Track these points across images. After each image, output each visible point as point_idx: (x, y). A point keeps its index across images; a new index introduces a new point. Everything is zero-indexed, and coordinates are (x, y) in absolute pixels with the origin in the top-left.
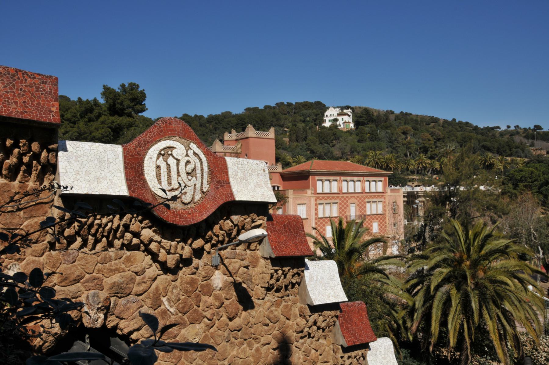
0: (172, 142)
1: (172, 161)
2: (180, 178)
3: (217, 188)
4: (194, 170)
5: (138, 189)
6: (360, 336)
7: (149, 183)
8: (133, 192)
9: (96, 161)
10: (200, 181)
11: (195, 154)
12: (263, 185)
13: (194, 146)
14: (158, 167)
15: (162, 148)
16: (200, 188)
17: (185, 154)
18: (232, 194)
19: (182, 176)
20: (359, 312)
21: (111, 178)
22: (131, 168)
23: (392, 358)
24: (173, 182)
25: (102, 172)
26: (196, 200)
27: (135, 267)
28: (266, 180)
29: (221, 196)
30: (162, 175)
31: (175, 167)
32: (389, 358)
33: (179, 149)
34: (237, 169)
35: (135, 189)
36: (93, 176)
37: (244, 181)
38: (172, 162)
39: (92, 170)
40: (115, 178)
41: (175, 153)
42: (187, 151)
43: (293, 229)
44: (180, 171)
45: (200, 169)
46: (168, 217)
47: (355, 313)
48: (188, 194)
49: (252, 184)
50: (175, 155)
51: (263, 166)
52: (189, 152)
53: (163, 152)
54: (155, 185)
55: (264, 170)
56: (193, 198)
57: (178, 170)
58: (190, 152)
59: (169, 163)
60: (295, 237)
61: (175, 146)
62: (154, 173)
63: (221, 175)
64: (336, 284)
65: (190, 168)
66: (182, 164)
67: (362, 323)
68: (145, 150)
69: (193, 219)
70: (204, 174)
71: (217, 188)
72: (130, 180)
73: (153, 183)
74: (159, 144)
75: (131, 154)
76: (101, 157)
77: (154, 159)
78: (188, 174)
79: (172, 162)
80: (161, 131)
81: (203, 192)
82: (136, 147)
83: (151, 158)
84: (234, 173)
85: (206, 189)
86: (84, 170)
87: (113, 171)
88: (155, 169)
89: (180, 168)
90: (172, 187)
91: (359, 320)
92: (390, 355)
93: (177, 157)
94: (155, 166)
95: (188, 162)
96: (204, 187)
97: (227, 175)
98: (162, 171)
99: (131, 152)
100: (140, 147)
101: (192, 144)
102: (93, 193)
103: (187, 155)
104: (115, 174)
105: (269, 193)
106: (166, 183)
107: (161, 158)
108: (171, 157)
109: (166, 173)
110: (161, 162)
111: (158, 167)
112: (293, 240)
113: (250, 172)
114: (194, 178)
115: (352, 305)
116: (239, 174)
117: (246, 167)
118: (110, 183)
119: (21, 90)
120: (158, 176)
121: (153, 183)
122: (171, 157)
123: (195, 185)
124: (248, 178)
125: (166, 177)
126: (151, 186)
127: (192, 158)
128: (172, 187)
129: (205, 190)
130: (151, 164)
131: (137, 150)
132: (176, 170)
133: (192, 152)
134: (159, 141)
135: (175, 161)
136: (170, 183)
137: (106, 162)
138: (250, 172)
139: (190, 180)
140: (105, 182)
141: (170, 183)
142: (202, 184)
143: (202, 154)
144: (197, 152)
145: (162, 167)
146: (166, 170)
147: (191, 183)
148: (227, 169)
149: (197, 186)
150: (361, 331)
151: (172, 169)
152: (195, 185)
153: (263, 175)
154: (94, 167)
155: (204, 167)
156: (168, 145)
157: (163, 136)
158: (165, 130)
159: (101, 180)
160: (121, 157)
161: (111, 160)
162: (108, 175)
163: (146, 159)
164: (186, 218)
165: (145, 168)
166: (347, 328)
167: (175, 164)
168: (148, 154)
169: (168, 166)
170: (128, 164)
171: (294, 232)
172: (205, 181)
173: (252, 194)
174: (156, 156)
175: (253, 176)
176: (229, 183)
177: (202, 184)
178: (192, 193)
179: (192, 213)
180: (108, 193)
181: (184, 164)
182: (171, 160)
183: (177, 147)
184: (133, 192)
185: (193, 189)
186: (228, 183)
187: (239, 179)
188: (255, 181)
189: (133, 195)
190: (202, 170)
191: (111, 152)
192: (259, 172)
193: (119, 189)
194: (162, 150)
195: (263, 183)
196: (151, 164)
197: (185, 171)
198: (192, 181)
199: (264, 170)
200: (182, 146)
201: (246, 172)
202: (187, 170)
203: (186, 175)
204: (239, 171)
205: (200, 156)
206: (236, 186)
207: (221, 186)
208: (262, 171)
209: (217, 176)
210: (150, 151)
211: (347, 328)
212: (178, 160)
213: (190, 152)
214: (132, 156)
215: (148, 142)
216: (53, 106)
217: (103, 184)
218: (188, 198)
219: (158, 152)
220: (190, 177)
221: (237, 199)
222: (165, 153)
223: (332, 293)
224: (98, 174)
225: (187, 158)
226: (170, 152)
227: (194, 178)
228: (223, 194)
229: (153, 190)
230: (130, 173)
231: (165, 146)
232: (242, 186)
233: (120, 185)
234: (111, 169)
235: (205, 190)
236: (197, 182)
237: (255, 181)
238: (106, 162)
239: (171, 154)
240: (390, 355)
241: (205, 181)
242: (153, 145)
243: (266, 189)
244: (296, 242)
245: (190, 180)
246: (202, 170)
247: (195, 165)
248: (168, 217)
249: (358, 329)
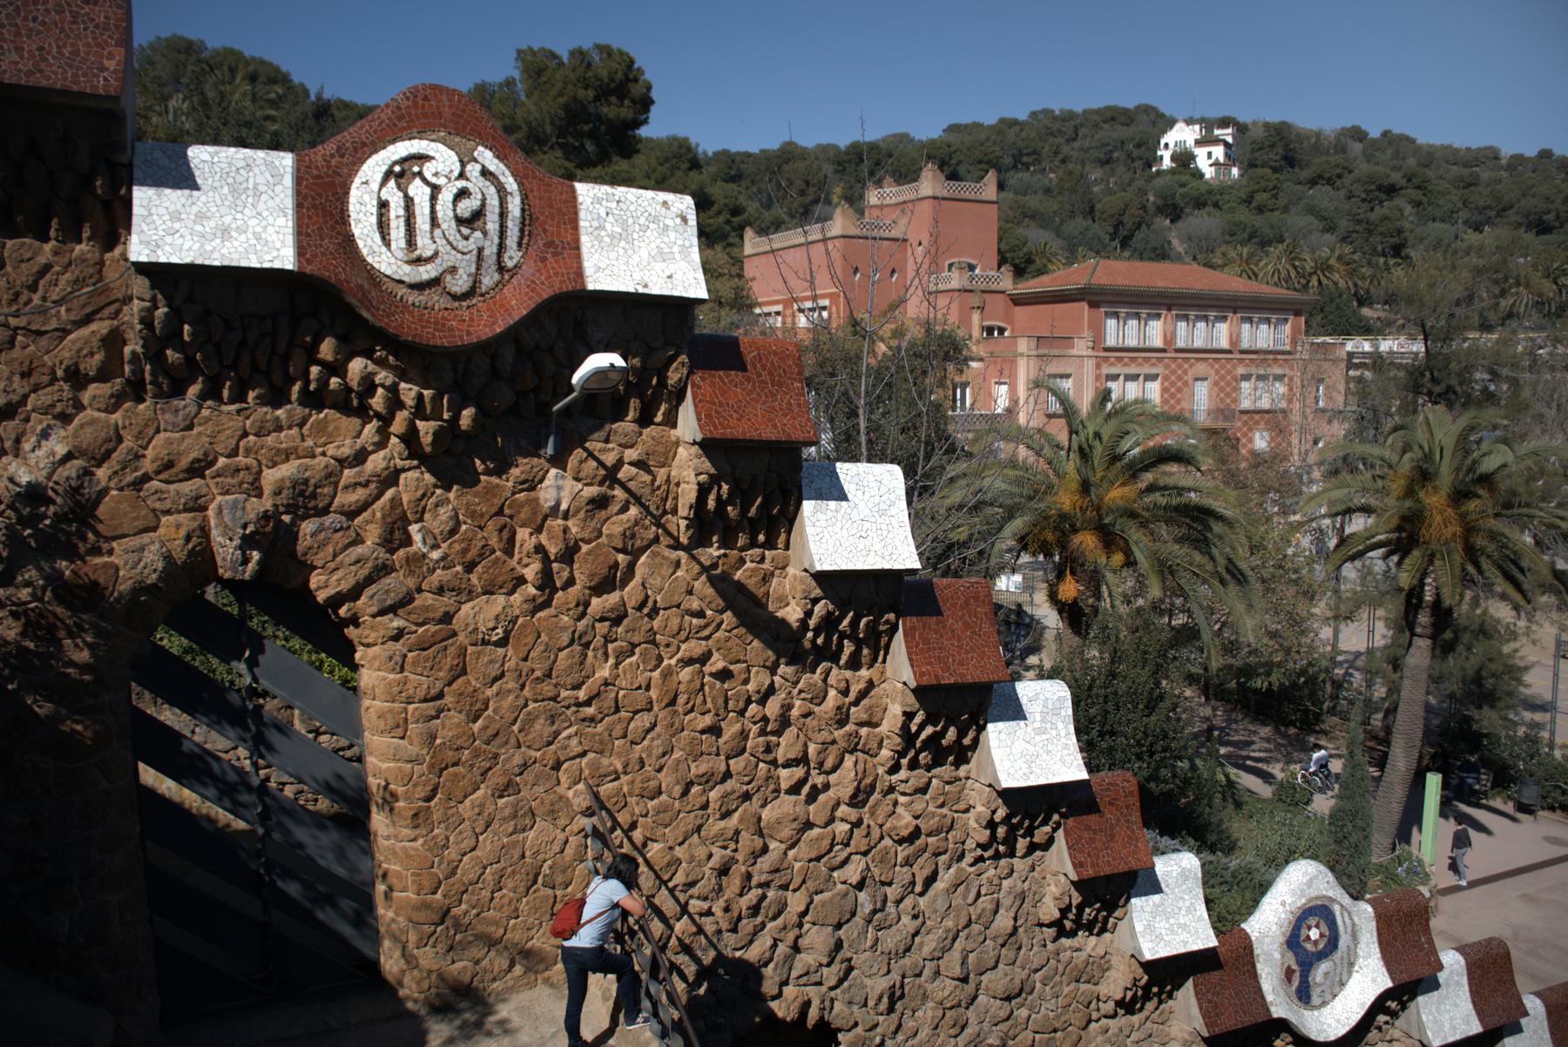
0: (424, 143)
1: (418, 191)
2: (437, 232)
3: (544, 260)
4: (478, 215)
5: (323, 254)
6: (961, 664)
7: (360, 244)
8: (309, 262)
9: (226, 190)
10: (496, 241)
11: (485, 173)
12: (678, 256)
13: (486, 156)
14: (383, 205)
15: (396, 157)
16: (494, 257)
17: (456, 173)
18: (580, 274)
19: (444, 226)
20: (967, 603)
21: (259, 229)
22: (315, 207)
23: (1063, 733)
24: (420, 242)
25: (239, 216)
26: (484, 289)
27: (339, 447)
28: (687, 243)
29: (549, 277)
30: (393, 224)
31: (427, 205)
32: (1054, 732)
33: (443, 159)
34: (603, 214)
35: (316, 256)
36: (212, 224)
37: (623, 244)
38: (419, 191)
39: (214, 209)
40: (270, 230)
41: (429, 170)
42: (463, 164)
43: (770, 374)
44: (440, 215)
45: (497, 210)
46: (401, 325)
47: (954, 605)
48: (461, 271)
49: (644, 253)
50: (428, 175)
51: (683, 207)
52: (469, 167)
53: (397, 169)
54: (376, 248)
55: (685, 220)
56: (476, 283)
57: (433, 212)
58: (473, 170)
59: (411, 193)
60: (773, 395)
61: (431, 153)
62: (374, 219)
63: (558, 225)
64: (895, 524)
65: (466, 208)
66: (446, 196)
67: (974, 632)
68: (354, 164)
69: (469, 333)
70: (510, 224)
71: (544, 260)
72: (308, 235)
73: (369, 242)
74: (391, 148)
75: (315, 172)
76: (239, 178)
77: (375, 186)
78: (460, 221)
79: (419, 191)
80: (400, 118)
81: (501, 268)
82: (332, 156)
83: (366, 183)
84: (595, 224)
85: (515, 261)
86: (195, 209)
87: (265, 214)
88: (374, 210)
89: (438, 208)
90: (417, 253)
91: (967, 626)
92: (1060, 725)
93: (434, 180)
94: (375, 202)
95: (462, 194)
96: (506, 256)
97: (576, 228)
98: (392, 215)
99: (317, 168)
100: (342, 156)
101: (480, 148)
102: (207, 263)
103: (462, 176)
104: (271, 220)
105: (691, 275)
106: (403, 244)
107: (392, 183)
108: (418, 181)
109: (402, 220)
110: (392, 194)
111: (383, 205)
112: (764, 403)
113: (642, 221)
114: (478, 234)
115: (949, 586)
116: (608, 227)
117: (632, 208)
118: (254, 242)
119: (35, 19)
120: (383, 227)
121: (369, 242)
122: (418, 181)
123: (480, 250)
124: (635, 236)
125: (402, 229)
126: (365, 252)
127: (475, 183)
128: (417, 253)
129: (510, 264)
130: (366, 198)
131: (333, 162)
132: (427, 211)
133: (478, 167)
134: (393, 141)
135: (428, 190)
136: (411, 242)
137: (250, 193)
138: (642, 221)
139: (466, 238)
140: (243, 238)
141: (411, 242)
142: (501, 247)
143: (507, 173)
144: (492, 168)
145: (392, 205)
146: (402, 212)
147: (471, 245)
148: (576, 213)
149: (487, 252)
150: (967, 652)
151: (418, 211)
152: (480, 250)
153: (681, 229)
154: (219, 202)
155: (510, 206)
156: (413, 151)
157: (404, 129)
158: (410, 115)
159: (234, 234)
160: (288, 181)
161: (262, 188)
162: (253, 222)
163: (354, 186)
164: (451, 329)
165: (351, 208)
166: (926, 641)
167: (427, 198)
168: (360, 174)
169: (409, 202)
170: (305, 198)
171: (773, 381)
172: (512, 242)
173: (637, 276)
174: (379, 177)
175: (649, 233)
176: (578, 248)
177: (501, 247)
178: (473, 270)
179: (471, 319)
180: (244, 264)
181: (451, 198)
182: (418, 191)
183: (437, 156)
184: (309, 262)
185: (474, 259)
186: (576, 246)
187: (607, 240)
188: (653, 245)
189: (308, 270)
190: (503, 215)
191: (263, 168)
192: (669, 222)
193: (275, 253)
194: (395, 163)
195: (676, 249)
196: (366, 198)
197: (451, 214)
198: (472, 240)
199: (685, 220)
200: (452, 153)
201: (630, 221)
202: (459, 211)
203: (453, 224)
204: (610, 218)
205: (502, 179)
206: (596, 256)
207: (555, 255)
208: (678, 220)
209: (545, 231)
210: (365, 167)
211: (926, 641)
212: (435, 189)
213: (473, 170)
214: (319, 177)
215: (364, 144)
216: (111, 56)
217: (236, 244)
218: (460, 282)
219: (385, 168)
220: (465, 231)
221: (590, 287)
222: (401, 173)
223: (877, 546)
224: (228, 220)
225: (461, 184)
226: (416, 169)
227: (478, 234)
228: (556, 274)
229: (369, 259)
230: (310, 217)
231: (404, 153)
232: (613, 255)
233: (278, 245)
234: (261, 207)
235: (510, 264)
236: (487, 243)
237: (653, 245)
238: (250, 193)
239: (420, 174)
240: (1060, 725)
241: (512, 242)
242: (376, 152)
243: (683, 264)
244: (773, 408)
245: (466, 238)
246: (503, 215)
247: (484, 200)
248: (401, 325)
249: (960, 647)
